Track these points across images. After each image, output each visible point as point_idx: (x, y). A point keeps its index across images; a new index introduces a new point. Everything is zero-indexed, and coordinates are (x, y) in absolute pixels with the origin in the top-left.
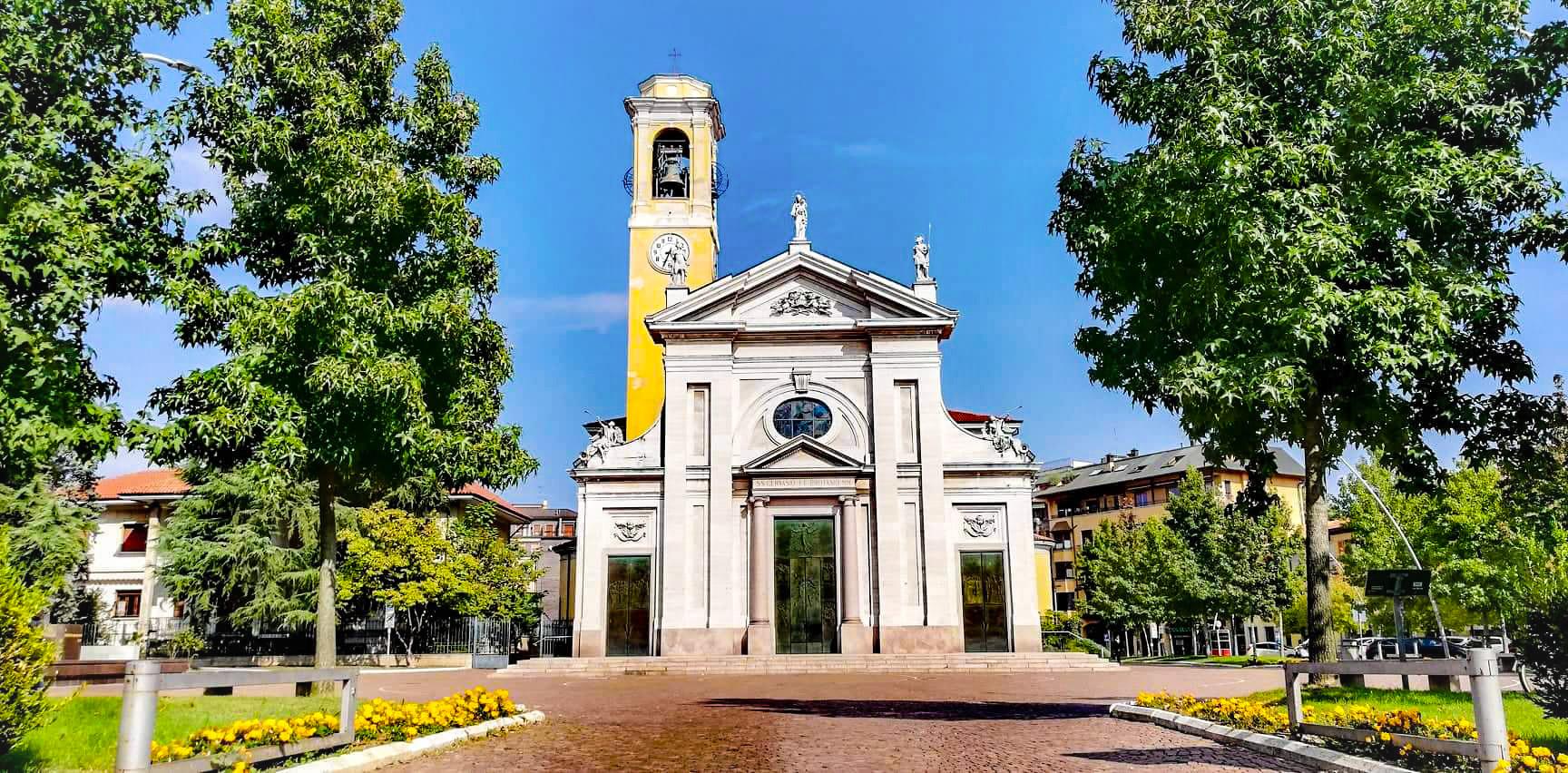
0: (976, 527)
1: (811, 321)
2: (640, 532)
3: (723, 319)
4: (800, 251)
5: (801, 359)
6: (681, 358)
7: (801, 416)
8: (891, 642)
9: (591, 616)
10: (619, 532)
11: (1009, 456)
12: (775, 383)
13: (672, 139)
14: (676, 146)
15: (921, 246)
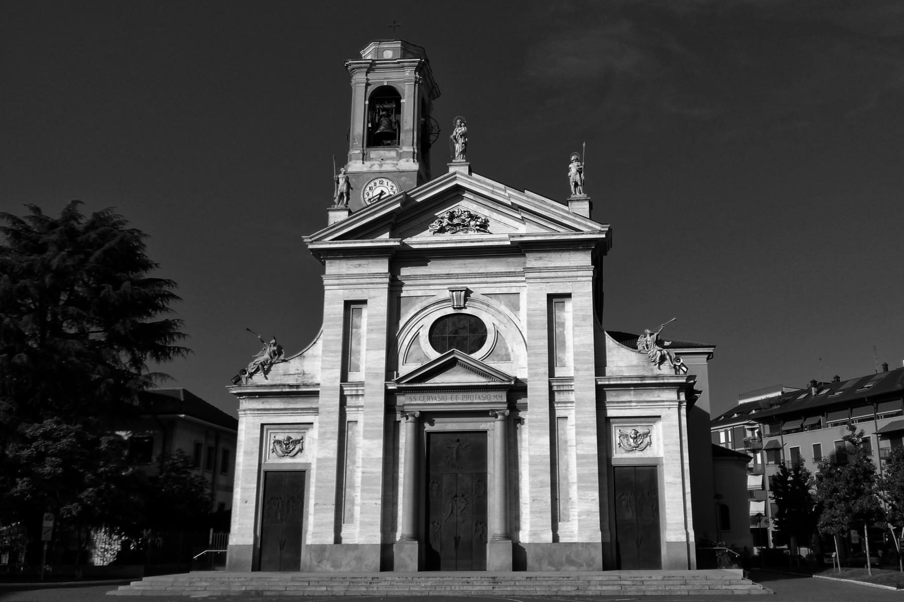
0: (631, 440)
1: (471, 238)
2: (298, 447)
3: (384, 239)
4: (459, 172)
5: (457, 276)
6: (339, 276)
7: (456, 332)
8: (539, 560)
9: (243, 529)
10: (278, 447)
11: (666, 369)
12: (432, 300)
13: (385, 99)
14: (390, 102)
15: (573, 167)
